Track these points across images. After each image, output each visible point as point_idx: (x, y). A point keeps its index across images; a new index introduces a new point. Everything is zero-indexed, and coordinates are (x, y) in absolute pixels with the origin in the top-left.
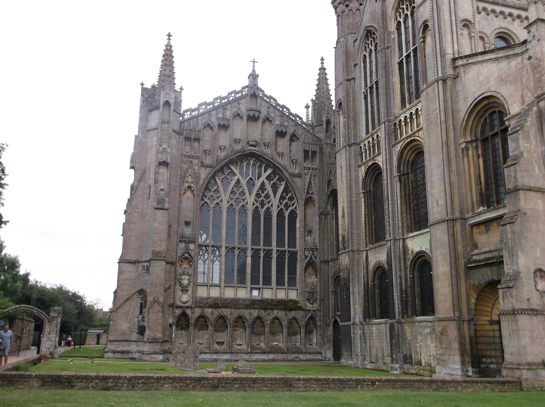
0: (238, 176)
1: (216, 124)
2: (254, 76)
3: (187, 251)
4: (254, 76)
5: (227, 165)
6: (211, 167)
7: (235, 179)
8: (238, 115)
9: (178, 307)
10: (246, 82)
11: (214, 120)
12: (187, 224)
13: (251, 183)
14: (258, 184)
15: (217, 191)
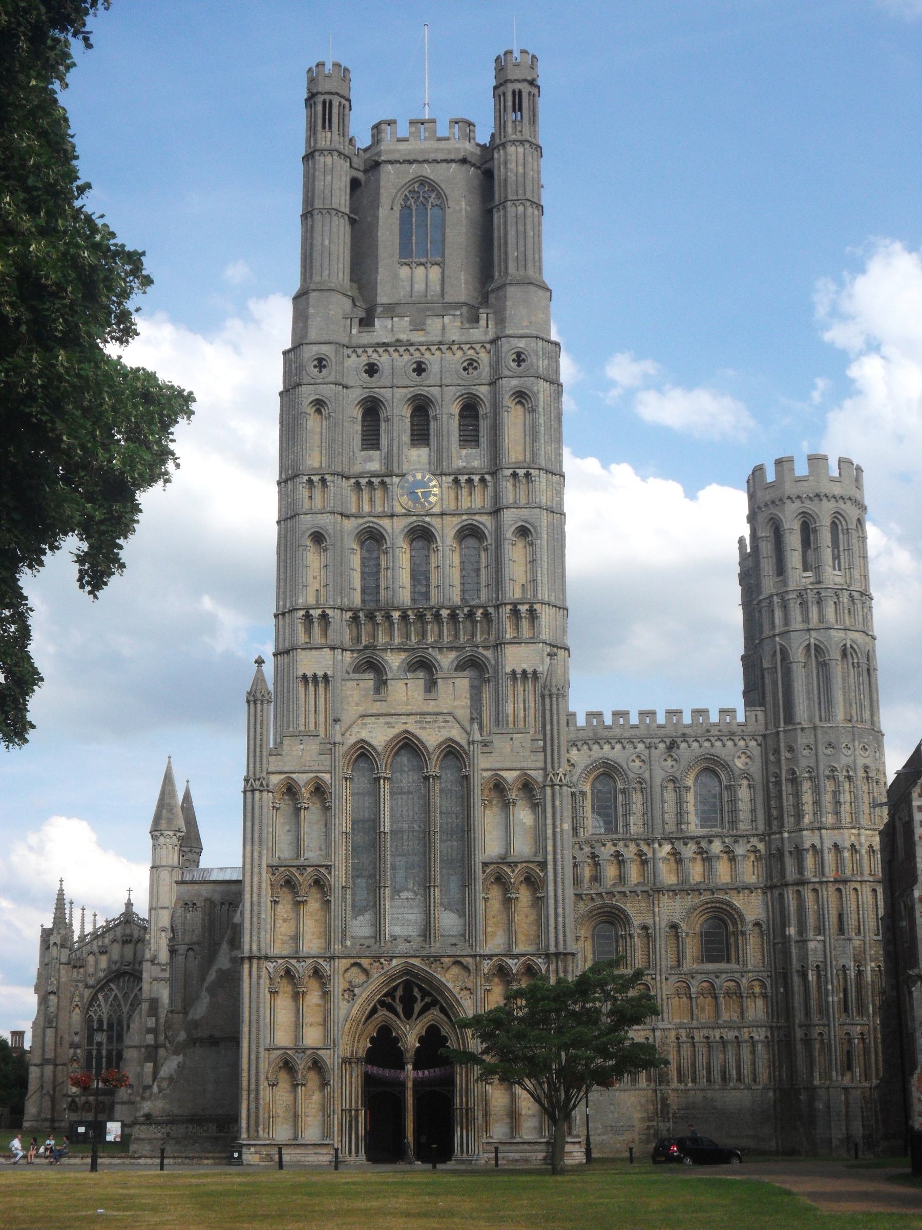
0: (116, 991)
1: (97, 951)
2: (129, 905)
3: (75, 1053)
4: (129, 905)
5: (107, 983)
6: (93, 987)
7: (114, 994)
8: (114, 941)
9: (69, 1096)
10: (123, 910)
11: (95, 948)
12: (76, 1034)
13: (126, 996)
14: (132, 996)
15: (99, 1006)
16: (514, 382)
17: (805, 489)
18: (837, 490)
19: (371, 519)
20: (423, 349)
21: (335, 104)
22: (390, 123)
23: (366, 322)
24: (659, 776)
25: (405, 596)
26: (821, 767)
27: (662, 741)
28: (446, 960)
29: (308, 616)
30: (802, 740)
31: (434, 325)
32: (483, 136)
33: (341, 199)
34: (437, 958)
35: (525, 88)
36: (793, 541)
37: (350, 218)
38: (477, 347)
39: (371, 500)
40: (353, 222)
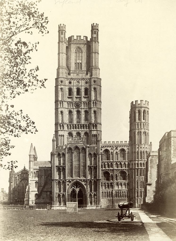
16: (94, 86)
17: (139, 106)
18: (144, 106)
19: (70, 109)
20: (79, 79)
21: (63, 32)
22: (73, 36)
23: (69, 74)
24: (115, 152)
25: (75, 122)
26: (139, 151)
27: (115, 146)
28: (82, 180)
29: (60, 125)
30: (137, 146)
31: (81, 75)
32: (89, 39)
33: (65, 51)
34: (81, 180)
35: (96, 31)
36: (137, 115)
37: (66, 54)
38: (88, 79)
39: (70, 106)
40: (67, 54)
